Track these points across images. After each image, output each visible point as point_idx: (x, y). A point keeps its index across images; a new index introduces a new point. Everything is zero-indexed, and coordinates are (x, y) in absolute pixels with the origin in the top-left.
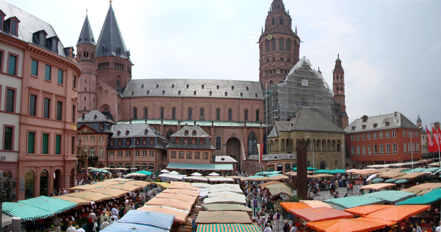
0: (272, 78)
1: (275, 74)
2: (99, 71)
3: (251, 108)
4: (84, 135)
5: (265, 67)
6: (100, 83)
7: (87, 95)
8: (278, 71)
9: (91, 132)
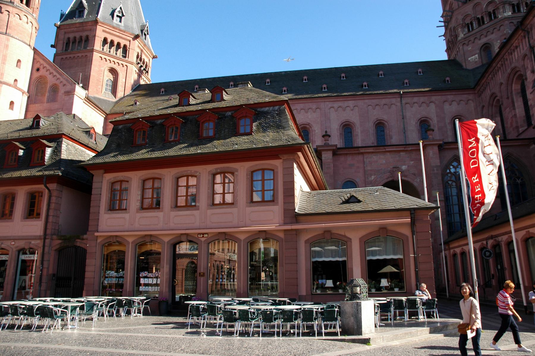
0: (486, 36)
1: (496, 20)
2: (64, 57)
3: (437, 116)
5: (460, 17)
6: (42, 67)
8: (504, 11)
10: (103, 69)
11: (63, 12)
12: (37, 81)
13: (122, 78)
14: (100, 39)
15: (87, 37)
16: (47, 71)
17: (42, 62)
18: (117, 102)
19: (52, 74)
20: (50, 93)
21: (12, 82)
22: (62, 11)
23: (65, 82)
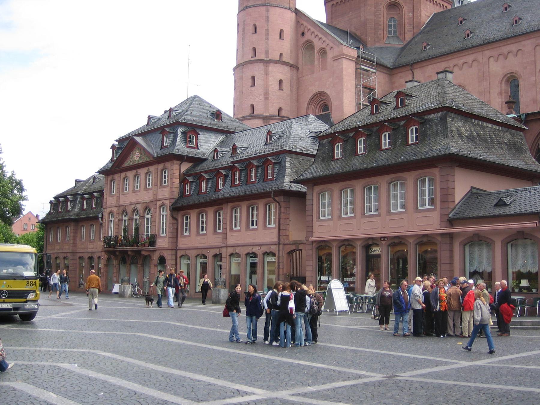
4: (133, 172)
6: (306, 31)
7: (257, 70)
9: (146, 159)
12: (304, 48)
16: (311, 35)
19: (317, 37)
20: (318, 61)
23: (331, 44)
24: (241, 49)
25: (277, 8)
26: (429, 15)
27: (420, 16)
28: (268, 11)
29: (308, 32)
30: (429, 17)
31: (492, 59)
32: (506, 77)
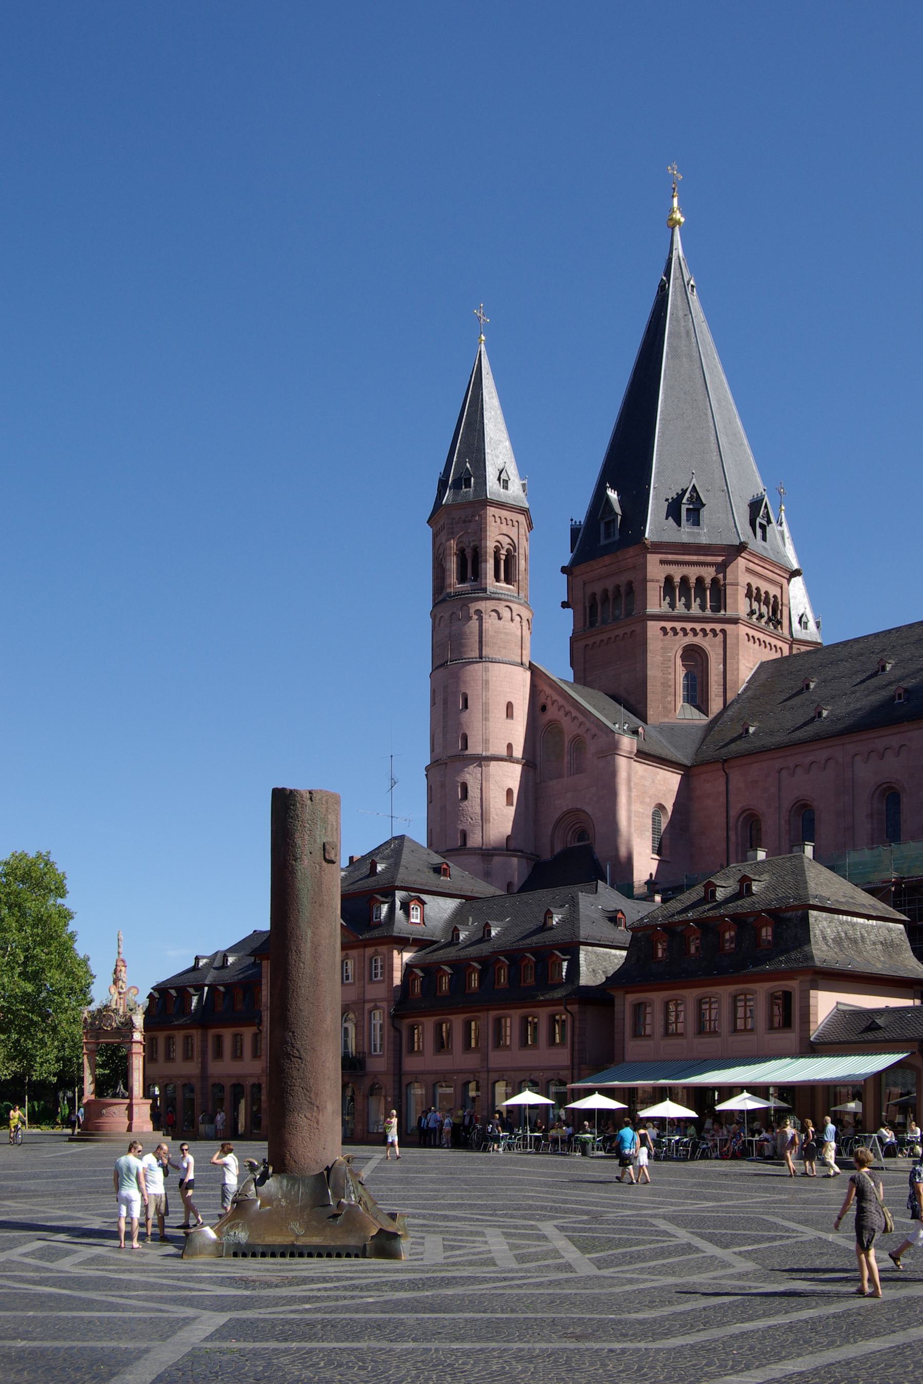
2: (590, 641)
6: (549, 702)
10: (671, 654)
11: (576, 522)
13: (716, 662)
14: (657, 585)
15: (630, 584)
16: (559, 710)
17: (548, 690)
18: (710, 727)
21: (504, 752)
22: (572, 520)
24: (441, 735)
25: (502, 665)
26: (751, 666)
27: (738, 669)
28: (487, 670)
29: (553, 704)
30: (752, 669)
31: (858, 758)
32: (881, 788)
